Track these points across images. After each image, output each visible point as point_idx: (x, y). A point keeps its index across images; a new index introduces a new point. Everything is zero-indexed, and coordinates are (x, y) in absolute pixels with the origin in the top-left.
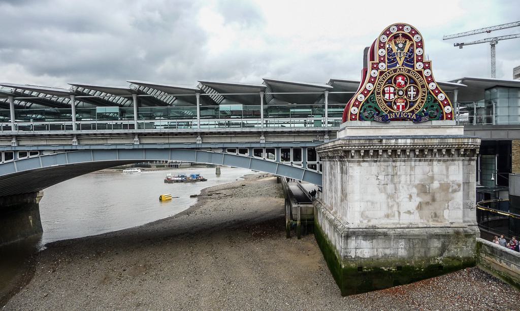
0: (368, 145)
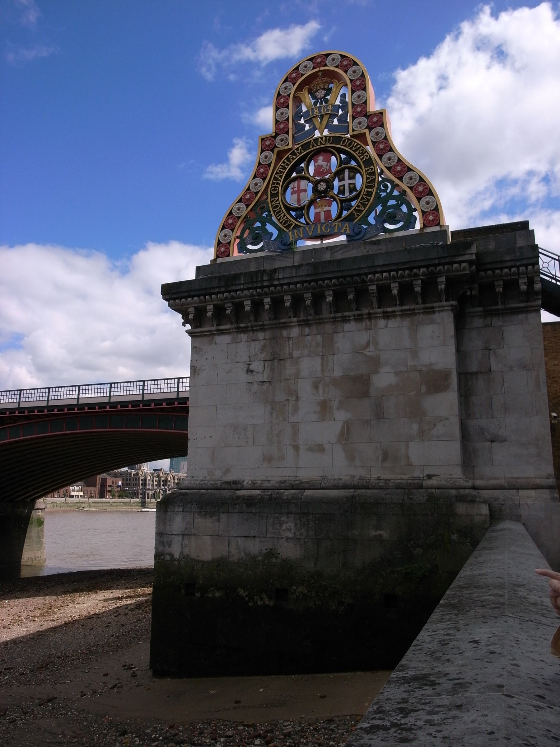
0: (216, 290)
